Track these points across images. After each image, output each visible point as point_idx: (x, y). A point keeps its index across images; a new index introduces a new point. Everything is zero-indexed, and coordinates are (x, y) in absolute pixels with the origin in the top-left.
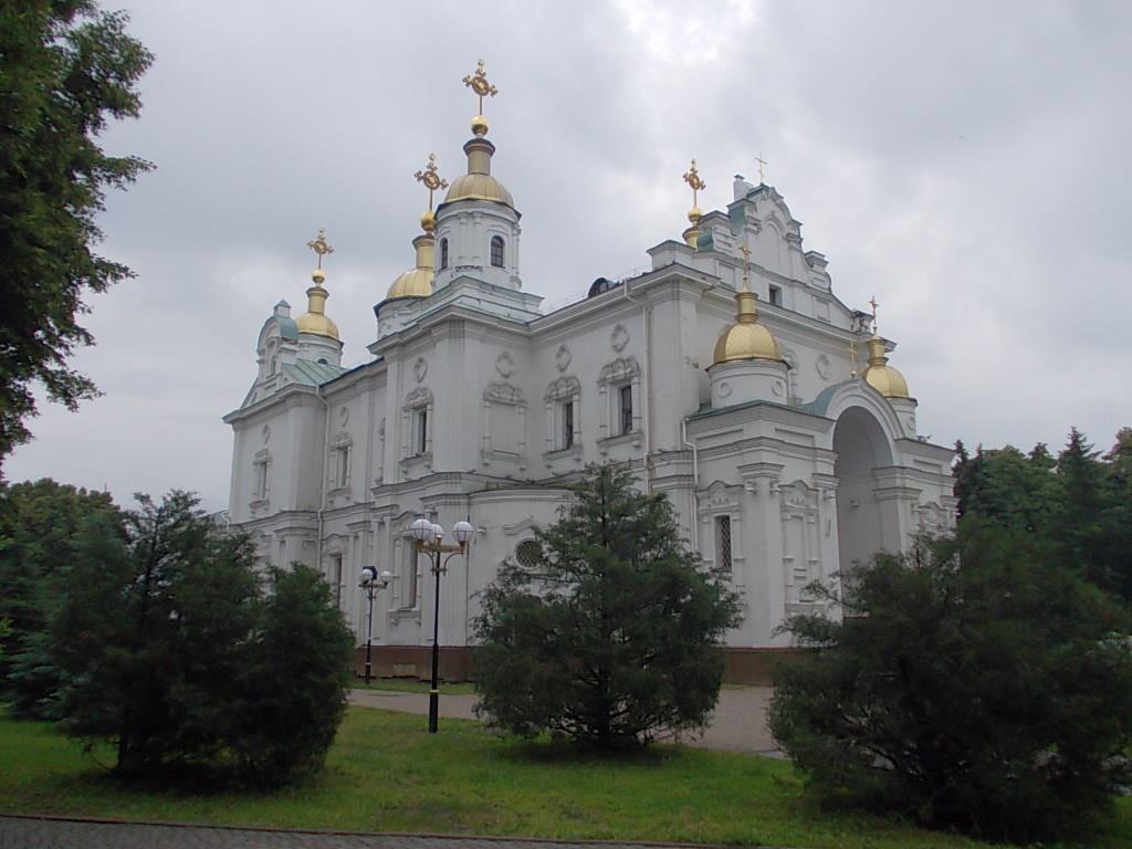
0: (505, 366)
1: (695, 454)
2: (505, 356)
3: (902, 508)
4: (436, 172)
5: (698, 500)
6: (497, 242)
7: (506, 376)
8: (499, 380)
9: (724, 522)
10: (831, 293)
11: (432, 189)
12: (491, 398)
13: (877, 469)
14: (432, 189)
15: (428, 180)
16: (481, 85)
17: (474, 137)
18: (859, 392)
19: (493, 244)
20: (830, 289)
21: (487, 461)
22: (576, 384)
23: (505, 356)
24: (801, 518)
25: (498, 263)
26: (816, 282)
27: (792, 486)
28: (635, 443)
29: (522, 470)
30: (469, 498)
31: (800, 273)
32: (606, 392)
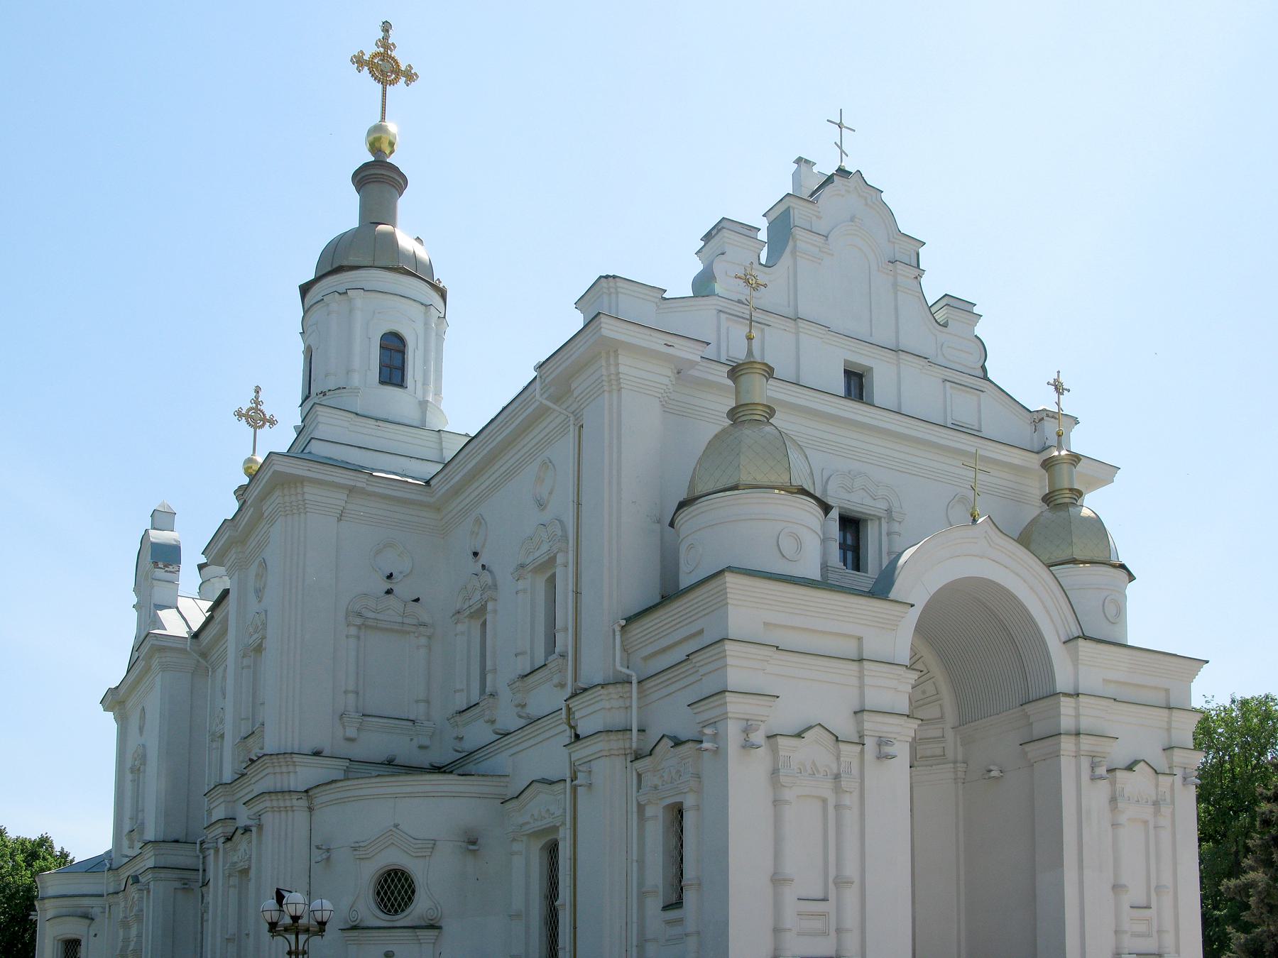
5: (639, 776)
9: (678, 812)
12: (358, 621)
21: (351, 732)
22: (490, 582)
27: (799, 735)
28: (556, 681)
29: (421, 747)
30: (310, 798)
31: (917, 335)
32: (525, 591)
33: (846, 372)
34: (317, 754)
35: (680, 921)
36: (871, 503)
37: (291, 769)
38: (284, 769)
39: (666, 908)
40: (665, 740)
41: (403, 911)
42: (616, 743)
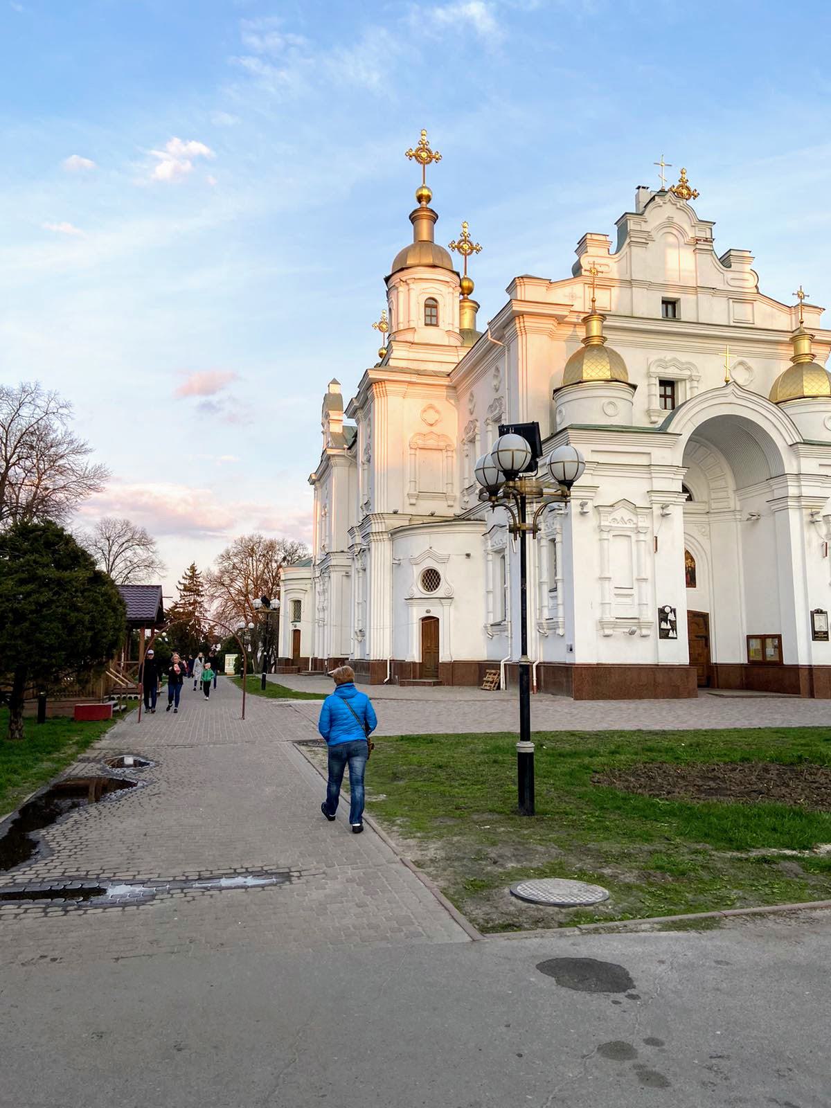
0: (431, 416)
2: (431, 407)
3: (795, 518)
4: (470, 239)
6: (433, 302)
7: (431, 425)
8: (427, 429)
10: (758, 293)
11: (466, 255)
13: (771, 478)
14: (466, 255)
15: (462, 247)
16: (424, 155)
17: (418, 206)
18: (732, 399)
19: (426, 306)
20: (756, 287)
23: (431, 407)
25: (434, 322)
26: (732, 283)
33: (663, 302)
34: (395, 513)
35: (556, 597)
36: (679, 372)
37: (383, 521)
38: (379, 521)
39: (550, 591)
41: (435, 589)
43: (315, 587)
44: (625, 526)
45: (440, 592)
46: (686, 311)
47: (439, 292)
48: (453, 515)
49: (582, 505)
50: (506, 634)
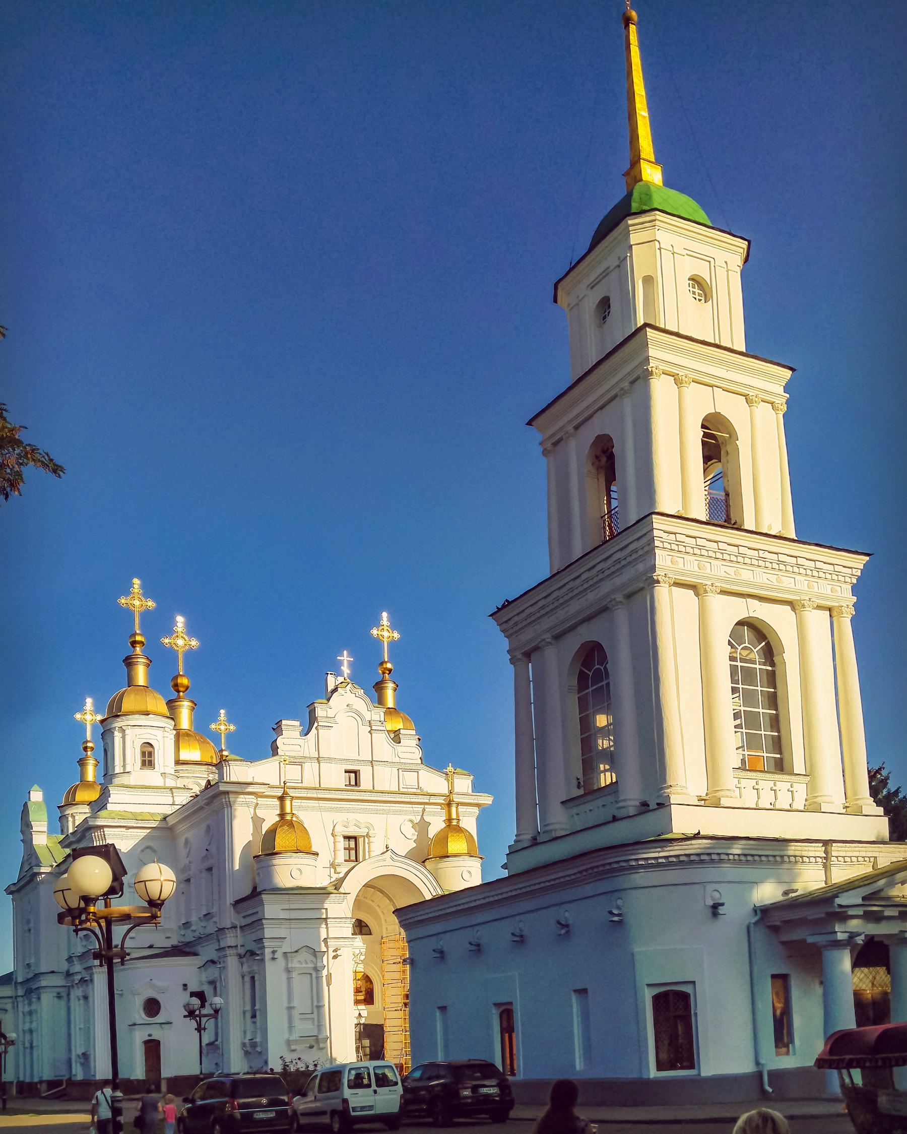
1: (238, 929)
24: (311, 974)
27: (296, 952)
40: (248, 953)
42: (233, 951)
43: (17, 1006)
44: (308, 966)
45: (160, 1018)
46: (365, 783)
47: (155, 738)
48: (170, 946)
49: (274, 952)
50: (218, 1052)
